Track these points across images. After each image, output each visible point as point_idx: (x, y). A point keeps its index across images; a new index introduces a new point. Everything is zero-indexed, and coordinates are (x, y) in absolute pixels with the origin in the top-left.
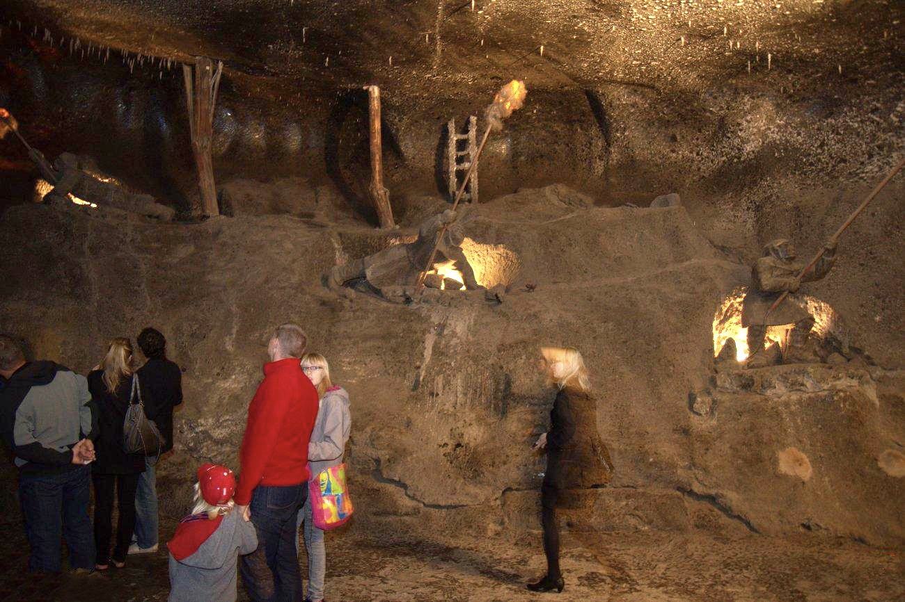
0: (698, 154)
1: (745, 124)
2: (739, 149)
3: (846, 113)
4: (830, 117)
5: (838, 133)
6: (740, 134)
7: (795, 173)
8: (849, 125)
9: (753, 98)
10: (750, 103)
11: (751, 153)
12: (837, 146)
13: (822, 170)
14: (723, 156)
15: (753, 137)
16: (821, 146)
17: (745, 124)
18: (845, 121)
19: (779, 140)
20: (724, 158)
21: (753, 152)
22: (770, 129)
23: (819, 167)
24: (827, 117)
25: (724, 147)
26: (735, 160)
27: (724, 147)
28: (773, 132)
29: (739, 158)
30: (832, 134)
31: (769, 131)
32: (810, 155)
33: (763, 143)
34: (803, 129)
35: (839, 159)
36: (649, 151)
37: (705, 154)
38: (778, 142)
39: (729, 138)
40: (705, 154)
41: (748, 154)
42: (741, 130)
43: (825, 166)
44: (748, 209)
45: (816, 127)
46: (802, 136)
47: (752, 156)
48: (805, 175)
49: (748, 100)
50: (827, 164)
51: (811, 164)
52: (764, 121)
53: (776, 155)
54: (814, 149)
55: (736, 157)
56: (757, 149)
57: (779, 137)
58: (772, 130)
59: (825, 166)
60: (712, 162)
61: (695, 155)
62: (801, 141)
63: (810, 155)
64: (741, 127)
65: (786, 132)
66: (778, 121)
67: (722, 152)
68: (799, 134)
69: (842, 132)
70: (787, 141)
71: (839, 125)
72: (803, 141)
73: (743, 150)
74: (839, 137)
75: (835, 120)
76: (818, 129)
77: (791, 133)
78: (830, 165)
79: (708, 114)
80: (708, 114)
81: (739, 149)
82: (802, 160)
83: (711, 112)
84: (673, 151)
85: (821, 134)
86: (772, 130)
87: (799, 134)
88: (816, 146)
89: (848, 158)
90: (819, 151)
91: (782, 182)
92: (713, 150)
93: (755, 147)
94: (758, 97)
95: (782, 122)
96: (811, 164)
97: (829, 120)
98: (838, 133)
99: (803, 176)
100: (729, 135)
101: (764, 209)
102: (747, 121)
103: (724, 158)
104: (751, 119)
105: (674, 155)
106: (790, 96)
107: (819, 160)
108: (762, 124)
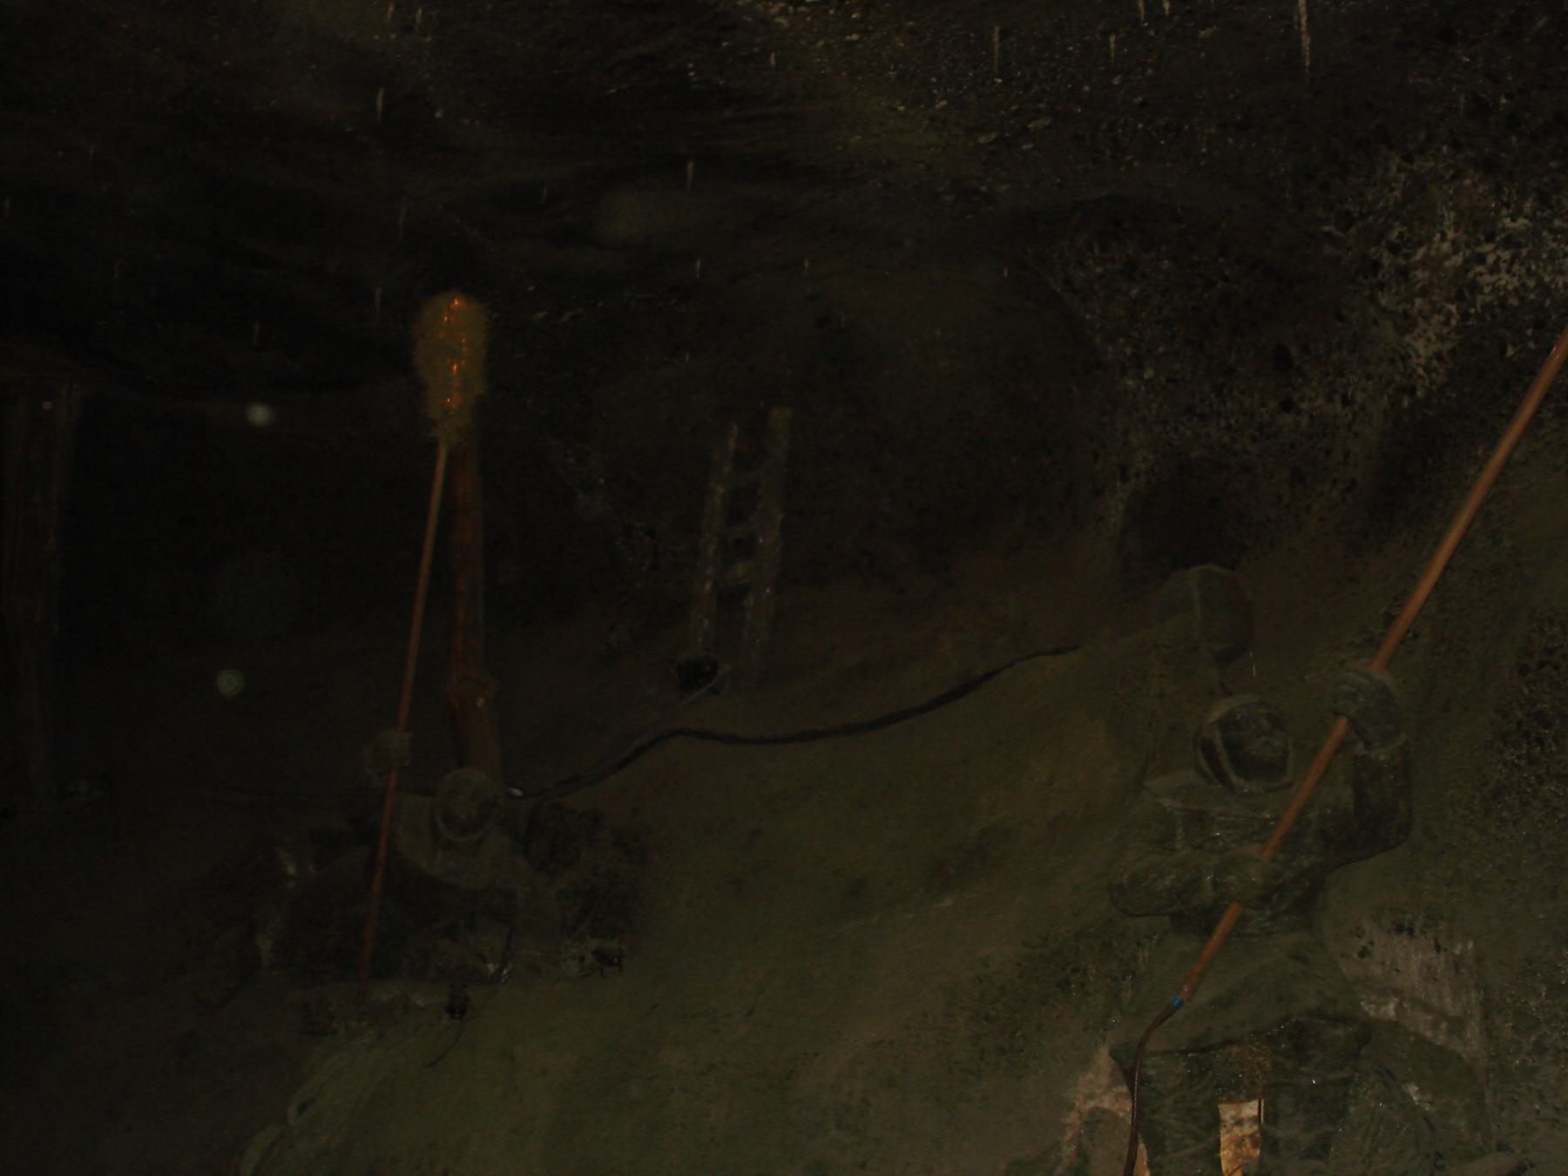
0: (1346, 401)
1: (1386, 259)
11: (1435, 363)
15: (1418, 302)
17: (1386, 259)
21: (1438, 356)
29: (1412, 391)
33: (1465, 316)
36: (1223, 423)
52: (1450, 234)
56: (1449, 345)
84: (1288, 406)
104: (1401, 235)
108: (1446, 246)
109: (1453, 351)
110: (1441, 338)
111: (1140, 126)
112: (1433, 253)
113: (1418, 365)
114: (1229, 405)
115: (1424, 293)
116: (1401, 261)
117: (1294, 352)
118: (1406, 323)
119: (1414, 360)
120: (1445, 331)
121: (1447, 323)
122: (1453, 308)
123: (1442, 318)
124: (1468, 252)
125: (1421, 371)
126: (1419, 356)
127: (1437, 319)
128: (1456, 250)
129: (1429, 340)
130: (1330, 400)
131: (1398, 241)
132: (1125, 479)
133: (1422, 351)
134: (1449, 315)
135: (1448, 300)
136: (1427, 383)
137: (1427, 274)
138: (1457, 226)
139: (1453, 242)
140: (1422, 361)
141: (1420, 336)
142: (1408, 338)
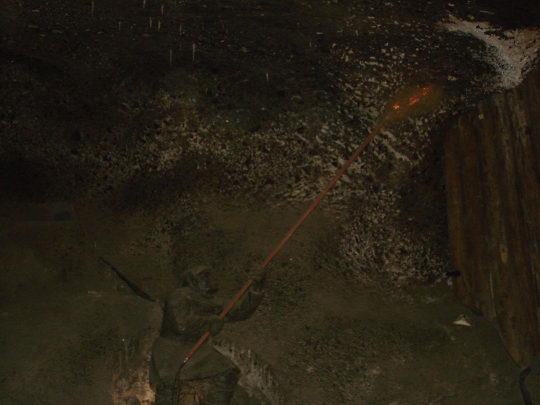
0: (105, 159)
1: (163, 125)
2: (155, 156)
3: (273, 129)
4: (256, 131)
5: (265, 151)
6: (157, 138)
7: (218, 192)
8: (276, 143)
9: (174, 97)
10: (170, 102)
11: (169, 163)
12: (264, 164)
13: (249, 189)
14: (135, 164)
15: (172, 143)
16: (248, 163)
17: (163, 125)
18: (271, 138)
19: (202, 150)
20: (137, 167)
21: (172, 161)
22: (192, 136)
23: (245, 187)
24: (253, 131)
25: (138, 153)
26: (150, 170)
27: (138, 153)
28: (195, 141)
29: (155, 168)
30: (258, 150)
32: (235, 172)
33: (184, 152)
34: (228, 142)
35: (265, 180)
36: (43, 149)
37: (114, 159)
38: (200, 153)
39: (144, 142)
40: (114, 159)
41: (166, 163)
42: (158, 133)
43: (251, 186)
44: (164, 230)
45: (242, 140)
46: (228, 149)
47: (170, 166)
48: (230, 194)
49: (169, 99)
50: (254, 183)
51: (237, 183)
52: (185, 126)
53: (198, 168)
54: (240, 165)
55: (151, 166)
56: (177, 159)
57: (201, 147)
58: (195, 137)
59: (251, 186)
60: (122, 170)
61: (101, 160)
62: (225, 155)
63: (235, 172)
64: (158, 130)
65: (210, 143)
66: (201, 129)
67: (135, 158)
68: (224, 147)
69: (269, 150)
70: (211, 153)
71: (266, 141)
72: (228, 155)
73: (160, 157)
74: (266, 154)
75: (262, 135)
76: (245, 144)
77: (214, 144)
78: (257, 186)
79: (120, 110)
80: (120, 110)
81: (155, 156)
82: (226, 177)
83: (124, 107)
84: (75, 152)
85: (248, 149)
86: (195, 137)
87: (224, 147)
88: (242, 162)
89: (275, 178)
90: (245, 168)
91: (204, 200)
92: (124, 155)
93: (175, 155)
94: (180, 97)
95: (205, 130)
96: (237, 183)
97: (256, 135)
98: (265, 151)
99: (228, 195)
100: (144, 138)
101: (182, 231)
102: (166, 122)
103: (137, 167)
104: (171, 120)
105: (75, 157)
106: (215, 102)
107: (245, 179)
108: (183, 129)
109: (178, 162)
110: (175, 156)
111: (88, 48)
112: (179, 130)
113: (163, 161)
114: (47, 144)
115: (174, 140)
116: (170, 128)
118: (162, 147)
119: (162, 159)
120: (177, 154)
121: (178, 152)
122: (181, 148)
123: (177, 150)
124: (188, 133)
125: (162, 163)
126: (164, 158)
127: (175, 150)
128: (186, 131)
129: (170, 155)
130: (97, 156)
131: (169, 122)
133: (166, 158)
134: (179, 150)
135: (180, 145)
136: (163, 167)
137: (176, 135)
138: (188, 124)
139: (186, 129)
140: (165, 160)
141: (168, 153)
142: (163, 152)
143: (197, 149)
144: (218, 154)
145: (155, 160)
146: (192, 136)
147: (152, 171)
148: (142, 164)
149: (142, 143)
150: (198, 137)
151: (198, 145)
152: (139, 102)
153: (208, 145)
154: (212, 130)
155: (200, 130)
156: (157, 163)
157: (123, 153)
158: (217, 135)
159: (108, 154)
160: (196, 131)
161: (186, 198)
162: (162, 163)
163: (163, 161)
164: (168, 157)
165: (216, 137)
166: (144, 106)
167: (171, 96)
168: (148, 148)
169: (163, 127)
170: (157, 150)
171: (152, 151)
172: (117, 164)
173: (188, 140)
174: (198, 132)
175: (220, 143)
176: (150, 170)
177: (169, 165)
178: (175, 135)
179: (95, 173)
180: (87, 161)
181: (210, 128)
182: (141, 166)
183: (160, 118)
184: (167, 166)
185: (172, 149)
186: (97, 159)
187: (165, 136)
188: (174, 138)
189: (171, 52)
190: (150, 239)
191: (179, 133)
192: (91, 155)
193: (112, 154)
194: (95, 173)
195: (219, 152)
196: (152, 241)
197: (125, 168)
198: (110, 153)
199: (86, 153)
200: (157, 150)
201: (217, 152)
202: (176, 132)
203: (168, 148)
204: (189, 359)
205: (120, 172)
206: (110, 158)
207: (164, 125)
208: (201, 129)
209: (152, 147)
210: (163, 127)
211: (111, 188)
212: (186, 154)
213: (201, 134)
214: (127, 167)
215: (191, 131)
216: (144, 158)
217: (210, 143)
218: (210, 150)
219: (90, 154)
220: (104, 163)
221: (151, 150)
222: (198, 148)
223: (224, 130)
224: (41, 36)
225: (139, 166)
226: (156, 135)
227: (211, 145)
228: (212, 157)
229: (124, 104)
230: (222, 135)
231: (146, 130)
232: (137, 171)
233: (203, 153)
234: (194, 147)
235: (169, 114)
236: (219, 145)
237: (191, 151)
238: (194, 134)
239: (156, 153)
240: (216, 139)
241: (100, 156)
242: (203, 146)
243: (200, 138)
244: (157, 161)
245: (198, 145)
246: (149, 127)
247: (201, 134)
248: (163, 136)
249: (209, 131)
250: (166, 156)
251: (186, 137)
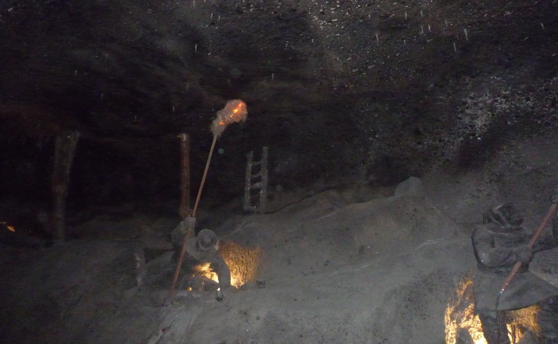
0: (440, 141)
1: (469, 101)
2: (471, 126)
6: (468, 112)
9: (473, 77)
10: (471, 82)
11: (483, 127)
14: (460, 137)
17: (469, 101)
19: (508, 109)
20: (462, 138)
21: (485, 125)
22: (496, 101)
25: (459, 128)
27: (459, 128)
28: (501, 103)
31: (496, 103)
33: (493, 115)
37: (446, 139)
38: (508, 111)
39: (460, 118)
40: (446, 139)
41: (480, 128)
42: (467, 108)
44: (491, 181)
47: (485, 130)
49: (469, 81)
52: (488, 95)
53: (509, 123)
55: (471, 135)
56: (488, 122)
57: (507, 106)
58: (499, 101)
60: (453, 144)
61: (438, 142)
64: (467, 105)
66: (504, 92)
67: (458, 133)
70: (518, 108)
73: (475, 125)
77: (519, 100)
79: (439, 103)
80: (439, 103)
81: (471, 126)
83: (441, 100)
84: (419, 143)
86: (499, 101)
92: (452, 134)
93: (486, 120)
95: (508, 92)
100: (460, 116)
102: (471, 98)
103: (462, 138)
104: (474, 95)
105: (420, 146)
108: (487, 98)
111: (397, 69)
112: (484, 99)
113: (478, 128)
115: (481, 109)
116: (475, 101)
117: (421, 130)
118: (474, 117)
120: (487, 118)
121: (488, 117)
122: (490, 113)
123: (487, 115)
124: (493, 99)
125: (478, 129)
126: (478, 125)
127: (485, 116)
129: (482, 121)
131: (473, 96)
132: (364, 163)
133: (480, 124)
134: (489, 114)
135: (488, 111)
136: (480, 132)
137: (482, 104)
138: (490, 92)
139: (489, 97)
140: (479, 126)
142: (475, 121)
143: (504, 109)
144: (524, 107)
145: (472, 129)
146: (496, 101)
147: (472, 138)
148: (464, 136)
149: (460, 120)
150: (502, 99)
151: (504, 106)
152: (450, 92)
153: (513, 102)
154: (513, 90)
155: (503, 94)
156: (474, 131)
157: (450, 132)
158: (519, 92)
159: (441, 136)
160: (499, 96)
161: (503, 150)
162: (478, 129)
163: (478, 128)
164: (481, 123)
165: (518, 94)
166: (454, 93)
167: (471, 77)
168: (465, 122)
169: (470, 102)
170: (471, 121)
171: (468, 123)
172: (449, 142)
173: (494, 105)
174: (501, 96)
175: (523, 98)
176: (471, 137)
177: (483, 129)
178: (481, 105)
179: (435, 153)
180: (428, 146)
181: (512, 89)
182: (463, 137)
183: (466, 97)
184: (483, 130)
185: (482, 116)
186: (435, 143)
187: (473, 108)
188: (481, 107)
189: (454, 44)
190: (481, 191)
191: (485, 103)
192: (431, 141)
193: (444, 136)
194: (435, 153)
195: (525, 105)
196: (483, 192)
197: (454, 142)
198: (442, 135)
199: (427, 141)
200: (471, 121)
201: (522, 106)
202: (481, 102)
203: (478, 117)
204: (505, 290)
205: (452, 147)
206: (443, 139)
207: (470, 101)
208: (504, 92)
209: (467, 120)
210: (470, 102)
211: (448, 160)
212: (495, 116)
213: (505, 97)
214: (455, 142)
215: (496, 97)
216: (465, 130)
217: (514, 100)
218: (515, 105)
219: (429, 141)
220: (440, 144)
221: (467, 122)
222: (505, 108)
223: (524, 86)
224: (364, 74)
225: (462, 137)
226: (466, 110)
227: (515, 102)
228: (519, 111)
229: (440, 97)
230: (523, 91)
231: (458, 109)
232: (462, 141)
233: (511, 111)
234: (501, 108)
235: (472, 91)
236: (523, 100)
237: (499, 113)
238: (498, 98)
239: (471, 124)
240: (519, 96)
241: (437, 140)
242: (509, 105)
243: (504, 100)
244: (474, 129)
245: (504, 106)
246: (460, 106)
247: (505, 97)
248: (471, 108)
249: (511, 91)
250: (479, 123)
251: (492, 103)
